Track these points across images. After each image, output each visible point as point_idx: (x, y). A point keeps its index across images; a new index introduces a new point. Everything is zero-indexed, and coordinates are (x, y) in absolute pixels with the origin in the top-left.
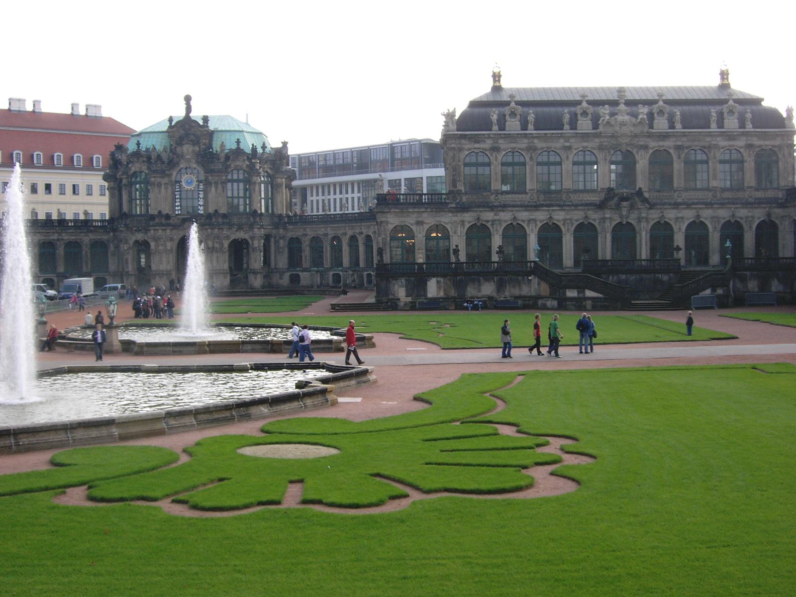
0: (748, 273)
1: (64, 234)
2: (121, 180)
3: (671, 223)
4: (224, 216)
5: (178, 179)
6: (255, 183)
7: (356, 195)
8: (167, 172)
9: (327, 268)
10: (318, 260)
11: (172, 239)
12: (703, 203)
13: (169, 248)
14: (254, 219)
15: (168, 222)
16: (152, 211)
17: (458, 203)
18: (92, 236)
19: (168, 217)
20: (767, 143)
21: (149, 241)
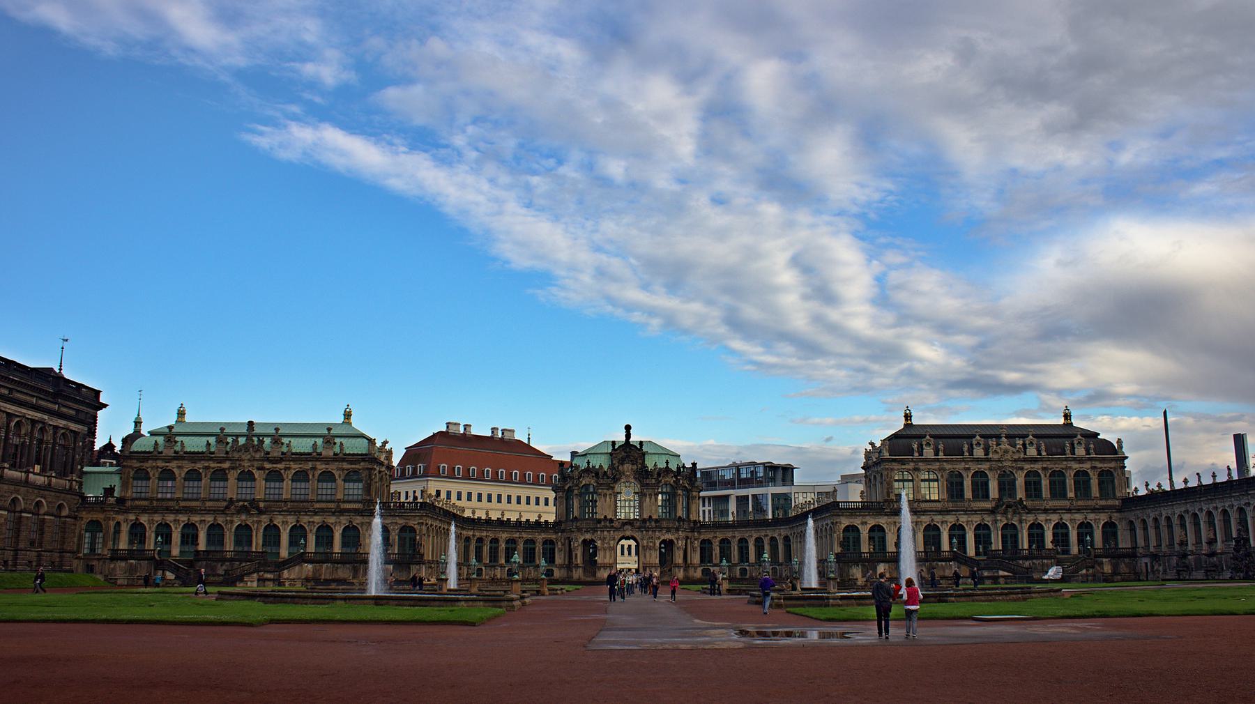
0: (1104, 560)
3: (1043, 524)
4: (657, 521)
6: (680, 495)
7: (707, 508)
8: (611, 485)
12: (1064, 509)
13: (612, 545)
17: (891, 509)
18: (544, 536)
19: (611, 521)
20: (1105, 465)
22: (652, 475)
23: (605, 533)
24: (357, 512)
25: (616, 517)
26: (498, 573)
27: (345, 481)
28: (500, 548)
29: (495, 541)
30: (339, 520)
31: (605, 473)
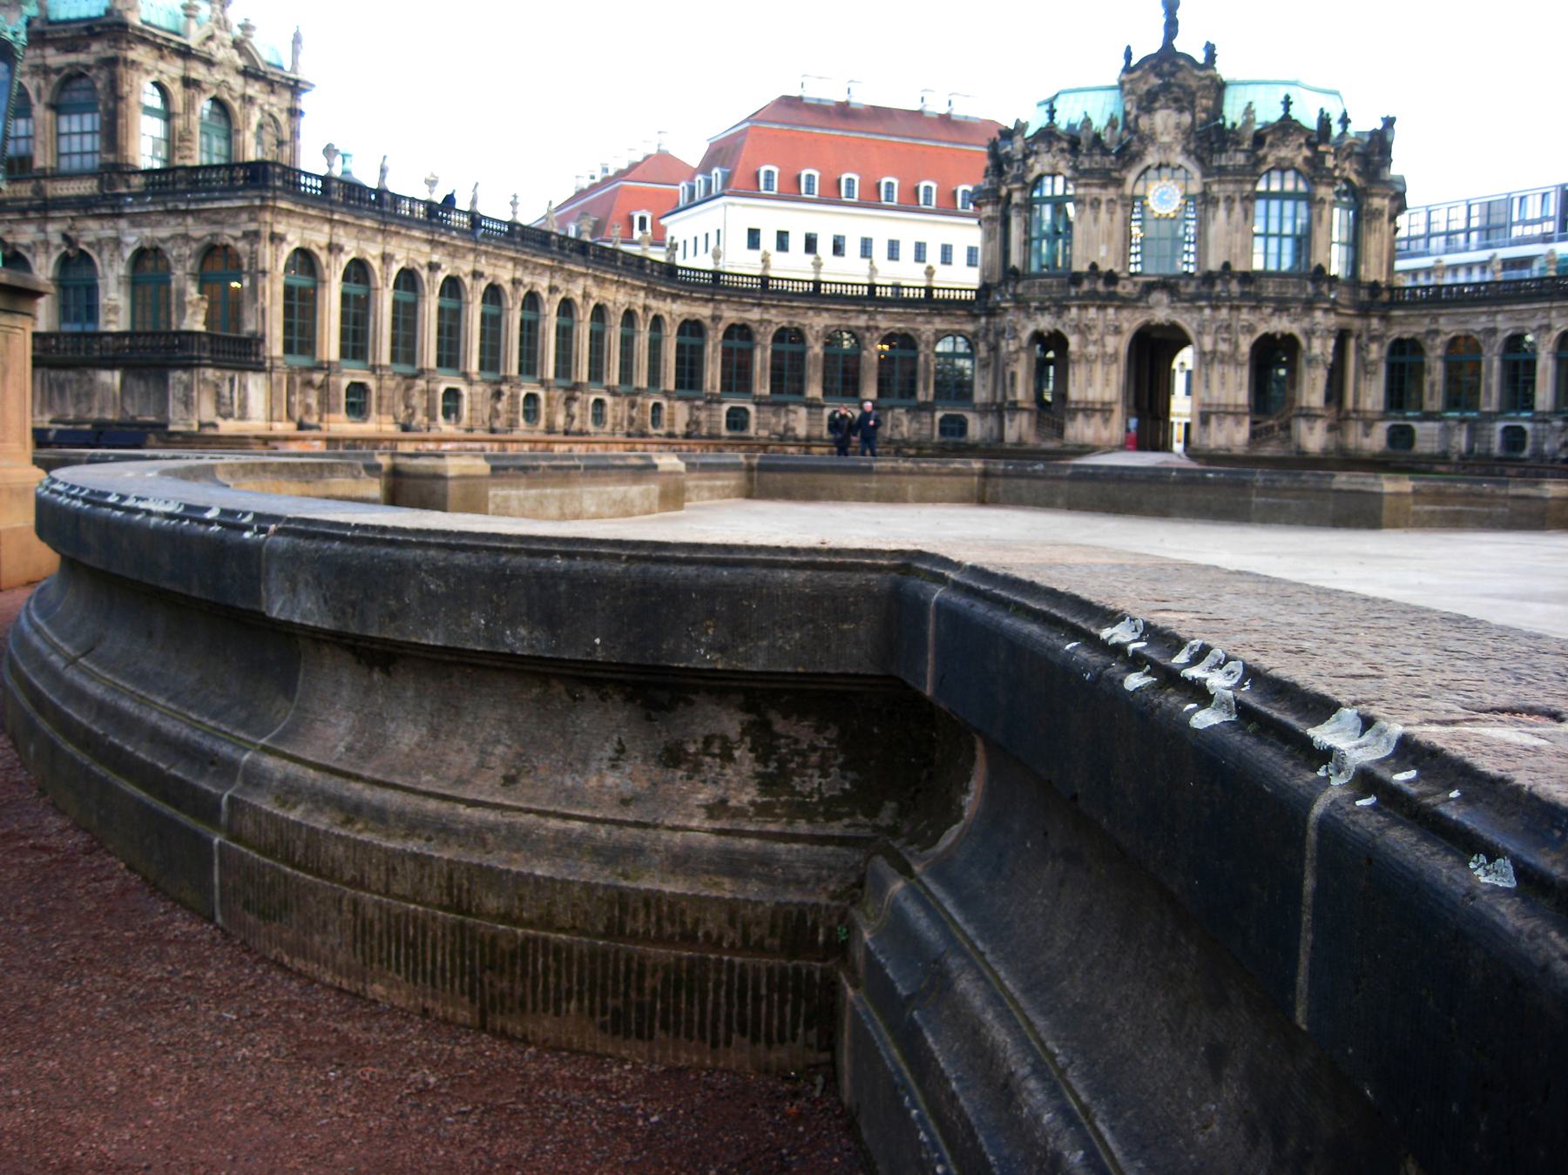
1: (879, 317)
2: (1009, 195)
4: (1248, 277)
5: (1139, 191)
6: (1322, 201)
8: (1115, 174)
9: (1490, 413)
10: (1461, 393)
11: (1117, 331)
13: (1110, 350)
14: (1317, 287)
15: (1112, 289)
16: (1080, 266)
18: (939, 324)
19: (1111, 278)
21: (1066, 331)
22: (1238, 143)
23: (1092, 312)
24: (84, 205)
25: (1125, 268)
26: (800, 422)
27: (57, 108)
28: (810, 354)
29: (789, 338)
30: (41, 236)
31: (1097, 137)
